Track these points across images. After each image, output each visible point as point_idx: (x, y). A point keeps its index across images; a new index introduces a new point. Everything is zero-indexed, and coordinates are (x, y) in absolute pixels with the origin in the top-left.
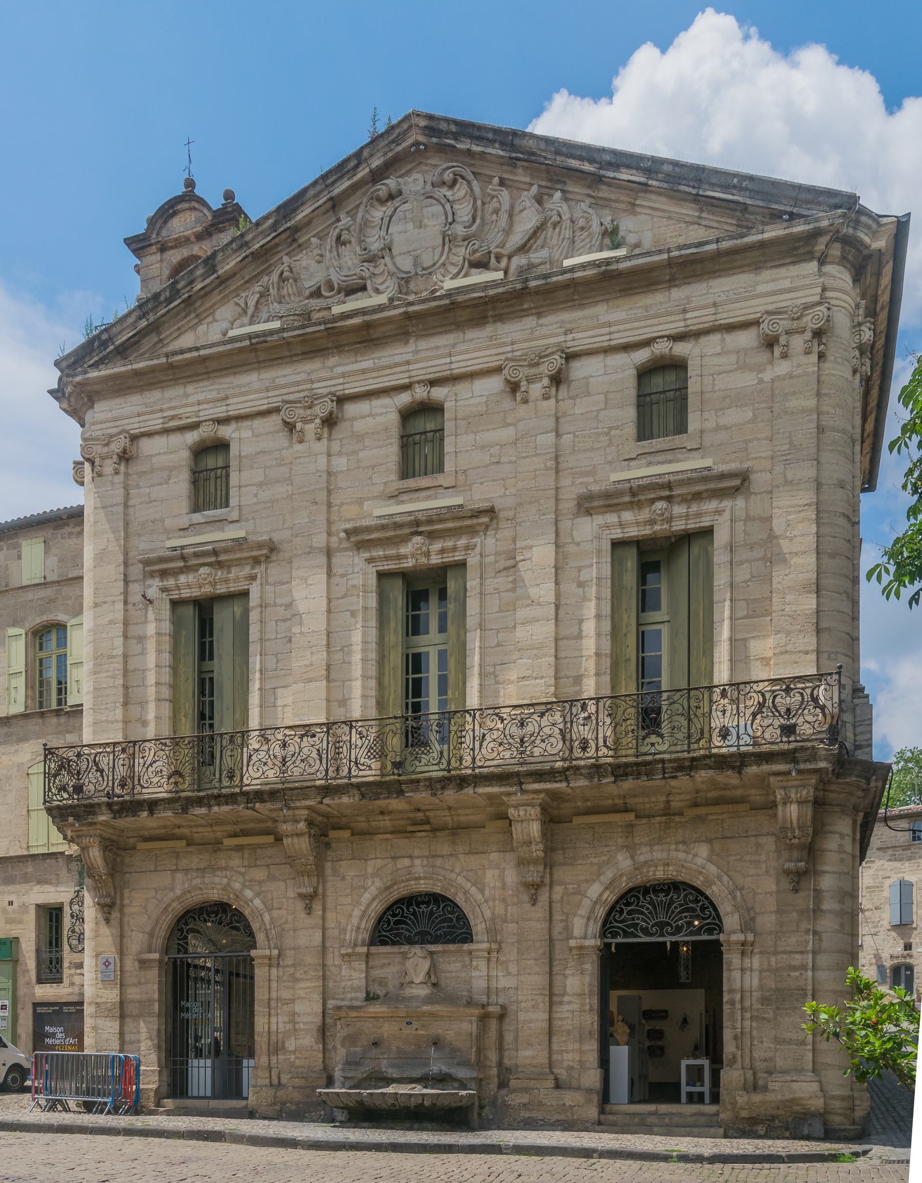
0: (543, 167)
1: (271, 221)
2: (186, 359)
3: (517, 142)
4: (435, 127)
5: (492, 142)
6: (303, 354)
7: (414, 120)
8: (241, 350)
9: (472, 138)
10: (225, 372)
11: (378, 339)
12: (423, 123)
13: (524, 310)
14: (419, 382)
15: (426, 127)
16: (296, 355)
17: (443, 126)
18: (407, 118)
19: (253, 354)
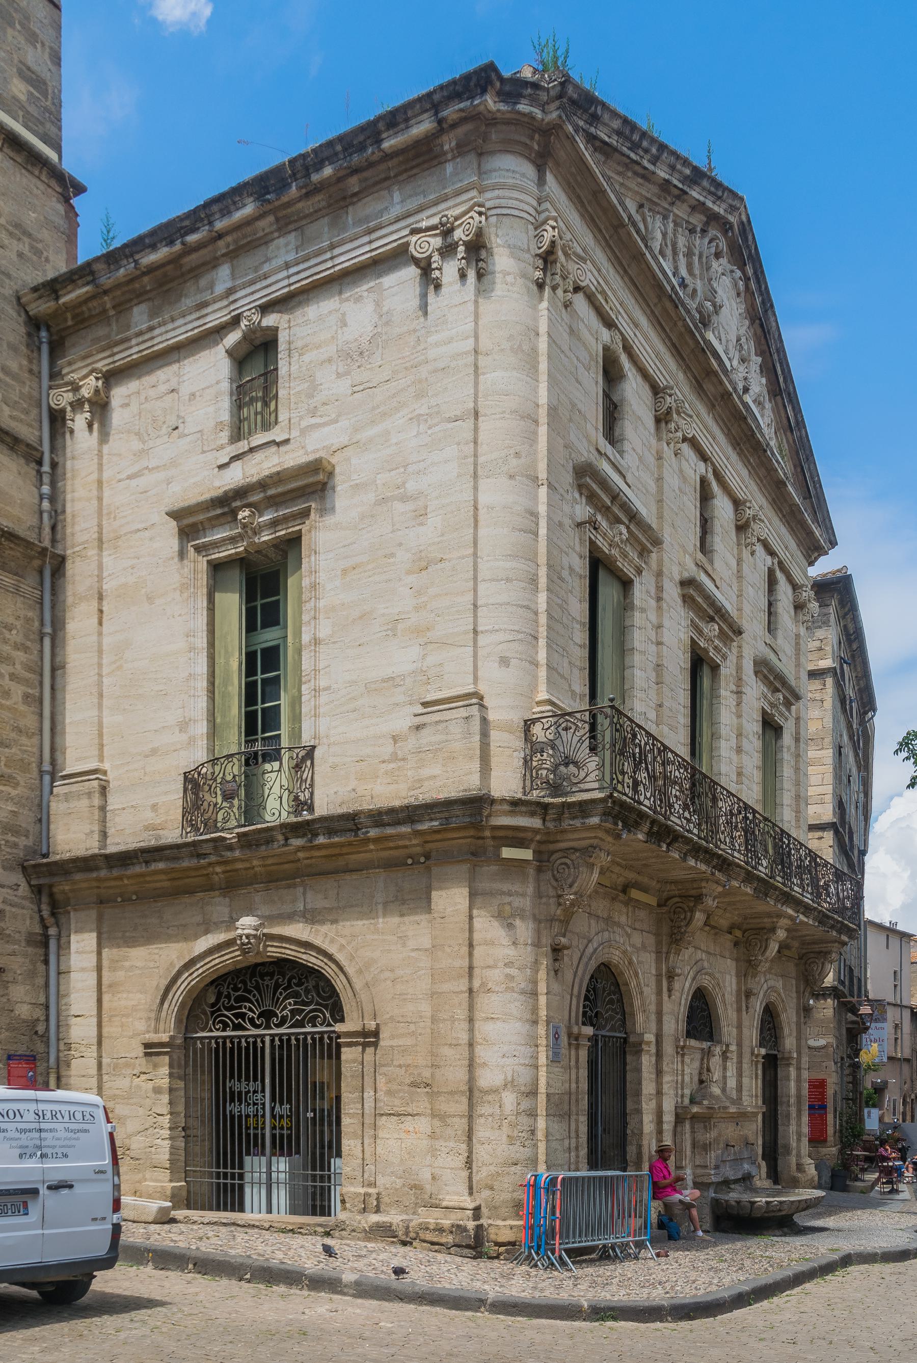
0: (765, 347)
1: (688, 172)
2: (635, 242)
3: (770, 312)
4: (746, 228)
5: (761, 294)
6: (674, 345)
7: (742, 209)
8: (660, 287)
9: (755, 273)
10: (633, 288)
11: (703, 390)
12: (744, 218)
13: (749, 461)
14: (713, 464)
15: (742, 223)
16: (670, 339)
17: (750, 237)
18: (742, 199)
19: (656, 301)
